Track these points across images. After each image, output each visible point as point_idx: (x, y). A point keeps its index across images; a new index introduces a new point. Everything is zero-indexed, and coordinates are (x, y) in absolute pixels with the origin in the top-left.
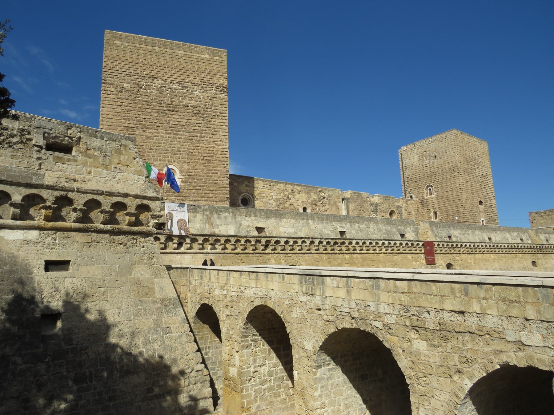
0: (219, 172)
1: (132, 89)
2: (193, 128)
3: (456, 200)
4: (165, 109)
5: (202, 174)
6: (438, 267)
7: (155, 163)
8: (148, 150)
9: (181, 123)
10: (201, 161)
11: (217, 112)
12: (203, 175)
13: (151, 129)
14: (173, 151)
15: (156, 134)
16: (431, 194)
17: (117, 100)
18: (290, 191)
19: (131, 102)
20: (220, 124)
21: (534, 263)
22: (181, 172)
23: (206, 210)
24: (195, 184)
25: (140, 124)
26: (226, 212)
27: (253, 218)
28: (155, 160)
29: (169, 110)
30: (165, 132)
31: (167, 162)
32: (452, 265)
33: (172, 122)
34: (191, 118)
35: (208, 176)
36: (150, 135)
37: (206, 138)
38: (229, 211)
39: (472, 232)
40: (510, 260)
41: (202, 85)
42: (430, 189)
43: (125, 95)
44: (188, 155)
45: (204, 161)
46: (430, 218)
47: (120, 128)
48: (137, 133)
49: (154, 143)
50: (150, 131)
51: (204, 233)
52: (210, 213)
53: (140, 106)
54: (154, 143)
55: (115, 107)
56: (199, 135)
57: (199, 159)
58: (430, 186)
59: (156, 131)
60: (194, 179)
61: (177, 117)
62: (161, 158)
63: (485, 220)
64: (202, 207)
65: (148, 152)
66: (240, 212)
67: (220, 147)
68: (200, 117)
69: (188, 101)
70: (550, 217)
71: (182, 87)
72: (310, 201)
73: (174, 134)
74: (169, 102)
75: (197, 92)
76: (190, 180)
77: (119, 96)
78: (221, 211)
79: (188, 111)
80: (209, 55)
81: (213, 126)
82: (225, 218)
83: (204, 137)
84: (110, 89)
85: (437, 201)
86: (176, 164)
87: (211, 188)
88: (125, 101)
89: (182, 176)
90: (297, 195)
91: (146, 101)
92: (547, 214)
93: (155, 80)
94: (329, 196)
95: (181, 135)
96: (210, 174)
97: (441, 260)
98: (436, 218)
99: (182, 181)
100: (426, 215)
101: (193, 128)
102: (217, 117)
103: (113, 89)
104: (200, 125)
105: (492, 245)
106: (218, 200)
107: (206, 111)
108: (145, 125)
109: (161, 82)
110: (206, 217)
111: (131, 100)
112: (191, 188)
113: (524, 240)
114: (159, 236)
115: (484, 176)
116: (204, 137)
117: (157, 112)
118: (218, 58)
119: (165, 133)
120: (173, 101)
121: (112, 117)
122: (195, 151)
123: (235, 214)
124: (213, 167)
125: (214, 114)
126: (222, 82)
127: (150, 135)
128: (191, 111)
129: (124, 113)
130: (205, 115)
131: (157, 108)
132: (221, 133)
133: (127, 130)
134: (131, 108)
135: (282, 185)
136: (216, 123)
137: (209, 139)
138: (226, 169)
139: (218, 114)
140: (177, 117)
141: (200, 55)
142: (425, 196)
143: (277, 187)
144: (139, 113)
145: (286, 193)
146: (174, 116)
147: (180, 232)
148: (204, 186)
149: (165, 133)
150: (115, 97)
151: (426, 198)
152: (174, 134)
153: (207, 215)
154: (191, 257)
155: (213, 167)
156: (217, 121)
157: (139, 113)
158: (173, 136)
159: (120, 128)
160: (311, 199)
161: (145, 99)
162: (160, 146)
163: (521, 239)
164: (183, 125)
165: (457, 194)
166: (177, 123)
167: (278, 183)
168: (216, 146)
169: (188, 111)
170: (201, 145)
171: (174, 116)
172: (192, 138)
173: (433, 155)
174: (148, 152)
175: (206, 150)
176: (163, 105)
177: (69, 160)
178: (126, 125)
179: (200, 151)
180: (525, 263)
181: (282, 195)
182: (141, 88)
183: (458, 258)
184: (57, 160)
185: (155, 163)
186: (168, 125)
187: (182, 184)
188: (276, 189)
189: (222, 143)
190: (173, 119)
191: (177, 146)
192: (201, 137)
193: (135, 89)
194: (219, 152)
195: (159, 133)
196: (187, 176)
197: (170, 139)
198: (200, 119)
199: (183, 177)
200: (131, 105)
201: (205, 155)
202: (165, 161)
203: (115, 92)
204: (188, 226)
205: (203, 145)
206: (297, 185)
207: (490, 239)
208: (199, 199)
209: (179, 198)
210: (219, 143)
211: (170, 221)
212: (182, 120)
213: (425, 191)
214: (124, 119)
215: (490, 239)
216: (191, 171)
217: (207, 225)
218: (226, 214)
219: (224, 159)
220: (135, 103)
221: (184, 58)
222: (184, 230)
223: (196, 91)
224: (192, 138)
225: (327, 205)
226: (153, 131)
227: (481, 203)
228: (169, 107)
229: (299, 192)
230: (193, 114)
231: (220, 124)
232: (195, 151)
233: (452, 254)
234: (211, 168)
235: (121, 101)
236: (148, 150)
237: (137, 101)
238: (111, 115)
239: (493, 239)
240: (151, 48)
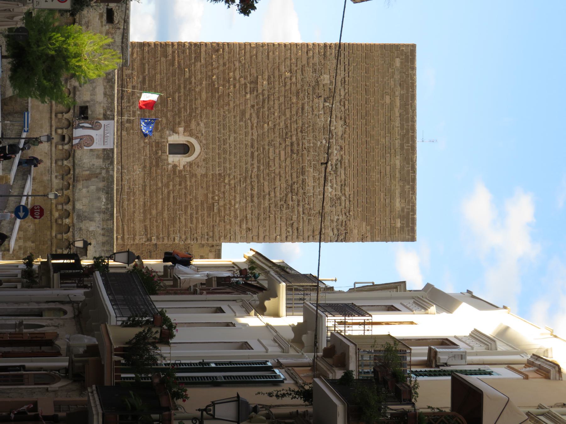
0: (194, 226)
1: (321, 86)
2: (266, 183)
4: (294, 138)
5: (189, 197)
7: (202, 125)
8: (222, 113)
9: (271, 163)
10: (210, 196)
11: (298, 224)
12: (188, 200)
13: (258, 118)
14: (225, 151)
15: (250, 124)
17: (299, 66)
19: (299, 86)
20: (278, 229)
22: (190, 164)
23: (108, 172)
24: (171, 187)
25: (264, 101)
26: (107, 199)
27: (101, 239)
28: (206, 125)
29: (292, 144)
30: (255, 137)
31: (204, 142)
33: (271, 149)
34: (283, 180)
35: (186, 207)
36: (248, 116)
37: (250, 204)
38: (108, 204)
41: (343, 198)
43: (309, 75)
44: (220, 174)
45: (210, 201)
47: (253, 71)
48: (248, 96)
49: (235, 122)
50: (254, 115)
51: (76, 167)
52: (104, 178)
53: (294, 100)
54: (235, 122)
55: (288, 63)
56: (255, 192)
57: (213, 192)
59: (255, 125)
60: (180, 185)
61: (283, 158)
62: (211, 133)
64: (111, 167)
65: (219, 114)
66: (108, 220)
67: (237, 228)
68: (286, 195)
69: (311, 175)
71: (336, 165)
73: (252, 153)
74: (307, 145)
75: (330, 190)
76: (178, 179)
77: (307, 68)
78: (107, 193)
79: (295, 175)
80: (403, 210)
82: (99, 198)
83: (252, 201)
84: (316, 56)
86: (203, 156)
87: (166, 212)
88: (299, 77)
89: (184, 166)
91: (303, 109)
93: (342, 122)
95: (252, 164)
96: (189, 212)
99: (175, 166)
101: (266, 183)
102: (289, 222)
103: (316, 60)
104: (272, 194)
106: (148, 223)
107: (298, 205)
108: (263, 107)
109: (340, 130)
110: (98, 171)
111: (302, 86)
112: (165, 180)
114: (72, 111)
116: (252, 201)
117: (287, 127)
118: (399, 225)
119: (252, 139)
120: (309, 151)
121: (271, 59)
122: (227, 187)
123: (104, 213)
124: (202, 216)
125: (295, 218)
126: (355, 231)
127: (248, 116)
128: (295, 180)
129: (280, 76)
130: (290, 203)
131: (294, 126)
132: (261, 230)
133: (251, 83)
134: (288, 87)
136: (278, 222)
137: (249, 209)
138: (199, 238)
139: (295, 225)
140: (283, 158)
141: (398, 195)
144: (282, 99)
146: (283, 153)
147: (76, 138)
148: (168, 200)
149: (252, 139)
150: (305, 62)
152: (252, 153)
153: (100, 173)
154: (46, 151)
155: (202, 216)
156: (283, 224)
157: (282, 99)
158: (249, 150)
159: (253, 71)
161: (306, 107)
162: (230, 131)
164: (269, 166)
166: (271, 158)
168: (238, 221)
169: (295, 175)
170: (238, 196)
171: (283, 153)
172: (249, 182)
174: (219, 114)
175: (230, 204)
176: (300, 134)
177: (102, 22)
178: (260, 80)
179: (227, 194)
182: (325, 101)
184: (101, 16)
185: (202, 125)
186: (266, 143)
187: (170, 166)
189: (244, 232)
190: (277, 151)
191: (232, 157)
192: (252, 196)
193: (321, 91)
194: (228, 227)
195: (252, 129)
196: (183, 173)
197: (244, 146)
198: (283, 194)
199: (182, 168)
200: (293, 88)
201: (221, 203)
202: (206, 139)
203: (311, 61)
204: (85, 148)
205: (238, 200)
208: (148, 194)
209: (148, 162)
210: (244, 226)
211: (90, 126)
212: (277, 165)
214: (269, 77)
216: (193, 180)
217: (88, 172)
218: (104, 200)
219: (217, 234)
220: (298, 93)
221: (388, 168)
222: (79, 143)
223: (332, 187)
224: (249, 182)
226: (255, 121)
228: (298, 145)
230: (290, 182)
231: (278, 229)
232: (227, 187)
234: (200, 213)
235: (299, 72)
236: (222, 113)
237: (301, 95)
238: (274, 58)
240: (397, 114)
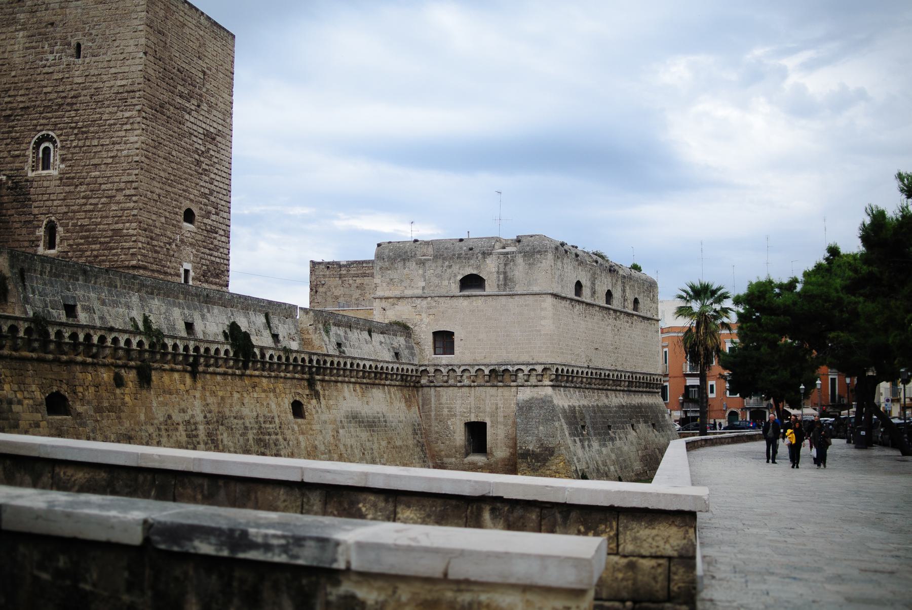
3: (120, 197)
16: (46, 166)
21: (298, 409)
32: (65, 399)
39: (141, 299)
40: (236, 395)
42: (47, 149)
46: (34, 243)
58: (47, 138)
63: (195, 268)
70: (359, 281)
85: (59, 190)
92: (353, 271)
98: (51, 245)
100: (24, 231)
105: (192, 345)
113: (281, 338)
115: (210, 137)
142: (28, 168)
151: (31, 174)
163: (275, 337)
165: (125, 178)
173: (74, 42)
180: (273, 406)
207: (189, 326)
213: (30, 153)
215: (189, 326)
227: (189, 216)
239: (199, 327)
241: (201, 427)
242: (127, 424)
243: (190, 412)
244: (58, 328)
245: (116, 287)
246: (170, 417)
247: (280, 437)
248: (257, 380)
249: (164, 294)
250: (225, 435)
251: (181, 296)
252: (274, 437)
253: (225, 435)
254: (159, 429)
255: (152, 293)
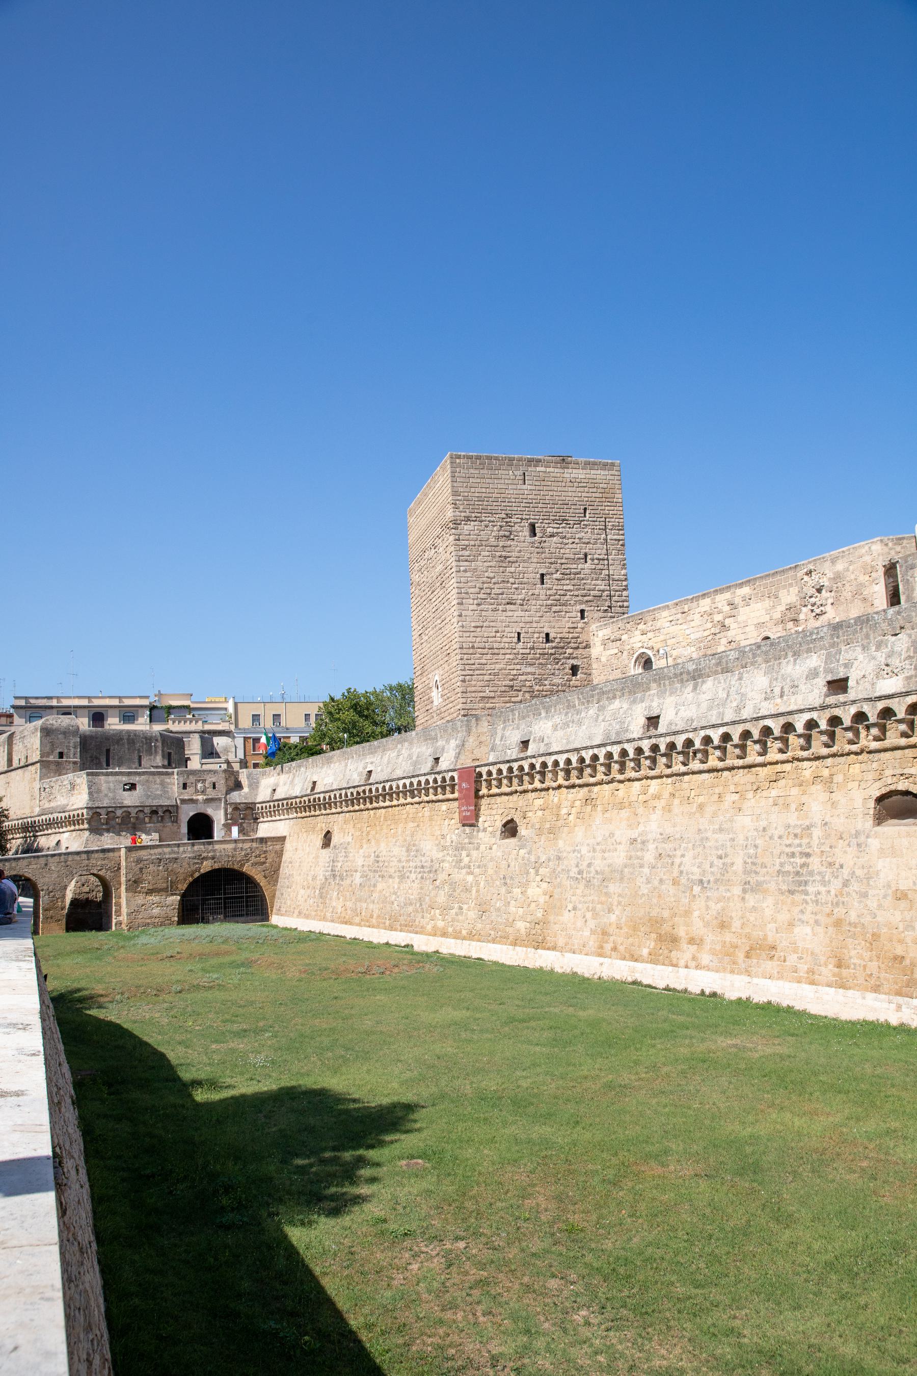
6: (485, 830)
10: (446, 659)
18: (727, 608)
72: (777, 615)
81: (448, 596)
90: (744, 613)
94: (837, 577)
97: (493, 814)
135: (707, 601)
143: (697, 610)
145: (718, 617)
160: (783, 608)
167: (697, 598)
181: (709, 625)
183: (539, 802)
188: (697, 616)
206: (741, 585)
225: (828, 608)
229: (747, 600)
233: (525, 791)
241: (651, 846)
242: (561, 843)
243: (641, 828)
244: (508, 765)
245: (574, 706)
246: (612, 835)
247: (815, 863)
248: (787, 767)
249: (630, 692)
250: (689, 855)
251: (654, 685)
252: (799, 861)
253: (689, 855)
254: (594, 850)
255: (614, 697)
